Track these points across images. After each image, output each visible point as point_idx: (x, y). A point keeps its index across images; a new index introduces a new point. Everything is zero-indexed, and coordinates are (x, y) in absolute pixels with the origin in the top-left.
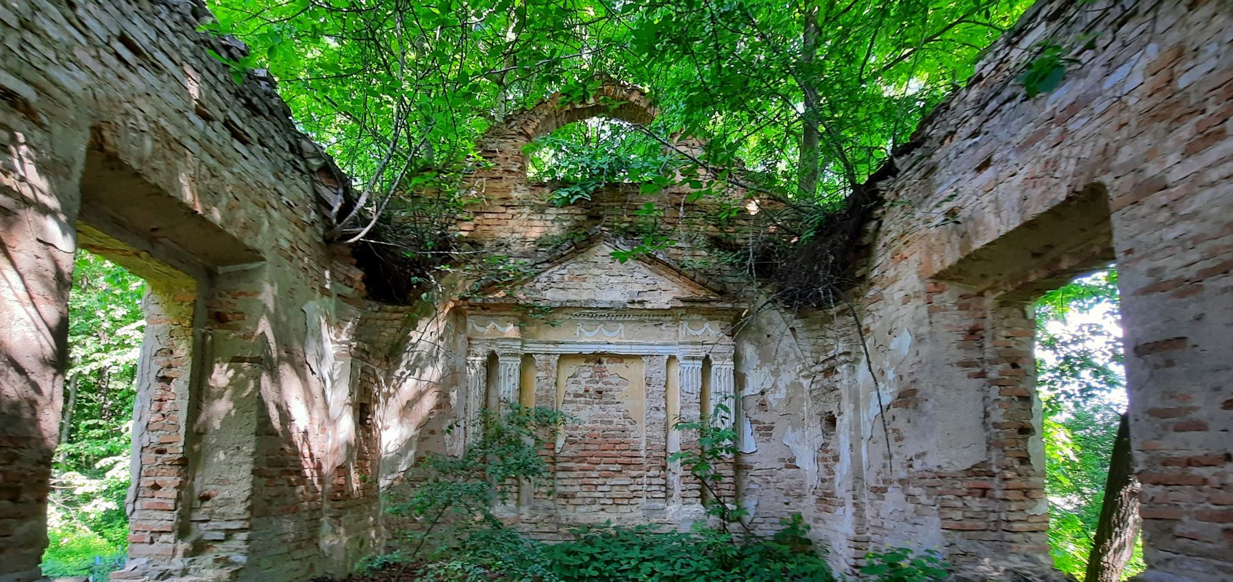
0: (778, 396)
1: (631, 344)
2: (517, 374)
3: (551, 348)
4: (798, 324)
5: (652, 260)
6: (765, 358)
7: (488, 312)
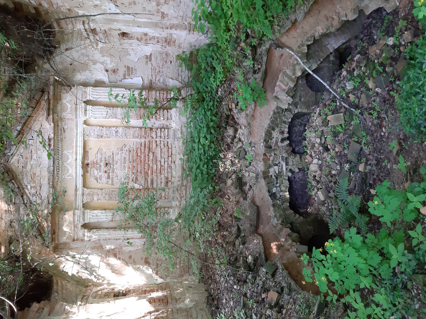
0: (109, 62)
1: (76, 146)
2: (95, 212)
3: (80, 192)
4: (63, 47)
6: (85, 67)
7: (56, 230)
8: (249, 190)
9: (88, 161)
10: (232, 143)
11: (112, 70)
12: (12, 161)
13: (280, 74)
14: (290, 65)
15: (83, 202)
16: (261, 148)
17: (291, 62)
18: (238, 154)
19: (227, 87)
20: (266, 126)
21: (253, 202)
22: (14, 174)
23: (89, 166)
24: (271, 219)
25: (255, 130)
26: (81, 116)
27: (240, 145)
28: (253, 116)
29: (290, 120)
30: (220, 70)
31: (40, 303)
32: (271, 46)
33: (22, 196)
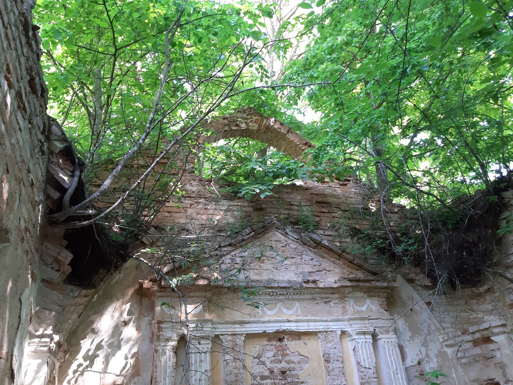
1: (308, 321)
3: (238, 329)
5: (318, 245)
9: (285, 341)
11: (422, 371)
12: (278, 234)
15: (222, 335)
22: (261, 235)
23: (279, 343)
26: (354, 326)
31: (69, 265)
33: (230, 245)
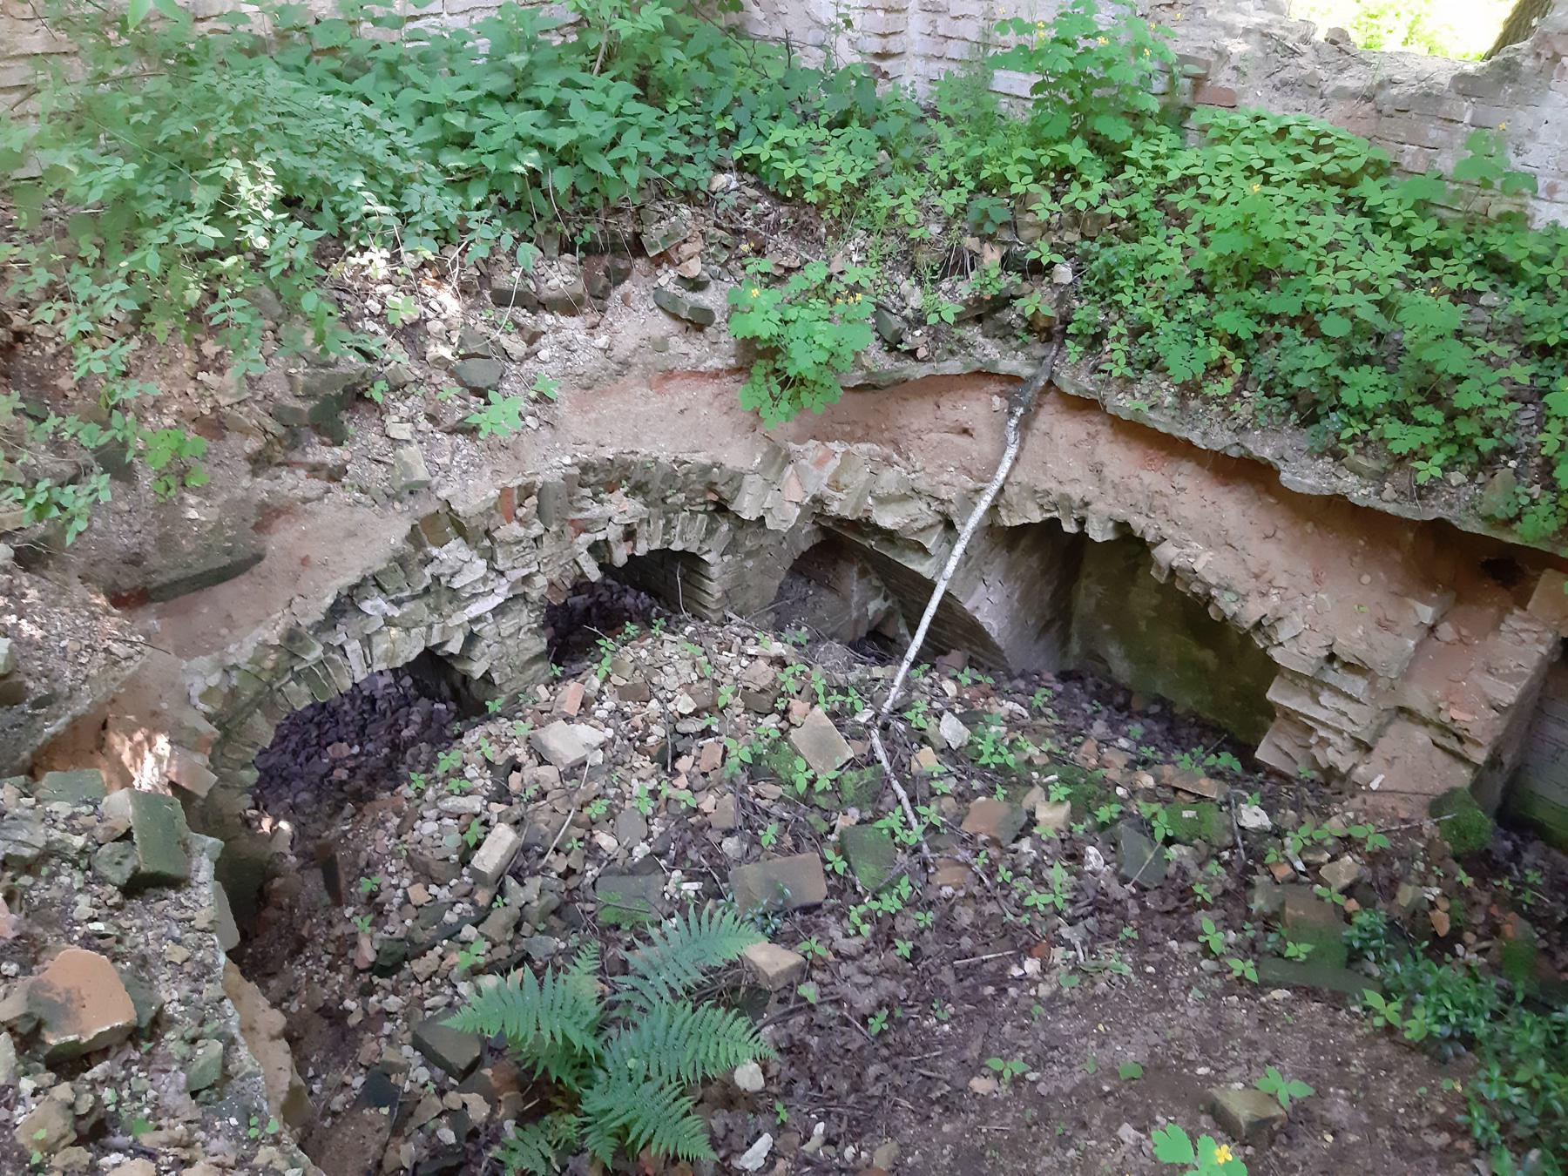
8: (315, 470)
10: (502, 299)
13: (880, 443)
14: (932, 475)
16: (551, 463)
17: (946, 477)
18: (474, 347)
19: (758, 219)
20: (644, 451)
21: (268, 515)
24: (206, 653)
25: (609, 407)
27: (517, 346)
28: (669, 375)
29: (677, 546)
30: (846, 170)
32: (1013, 379)
